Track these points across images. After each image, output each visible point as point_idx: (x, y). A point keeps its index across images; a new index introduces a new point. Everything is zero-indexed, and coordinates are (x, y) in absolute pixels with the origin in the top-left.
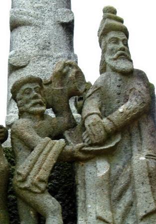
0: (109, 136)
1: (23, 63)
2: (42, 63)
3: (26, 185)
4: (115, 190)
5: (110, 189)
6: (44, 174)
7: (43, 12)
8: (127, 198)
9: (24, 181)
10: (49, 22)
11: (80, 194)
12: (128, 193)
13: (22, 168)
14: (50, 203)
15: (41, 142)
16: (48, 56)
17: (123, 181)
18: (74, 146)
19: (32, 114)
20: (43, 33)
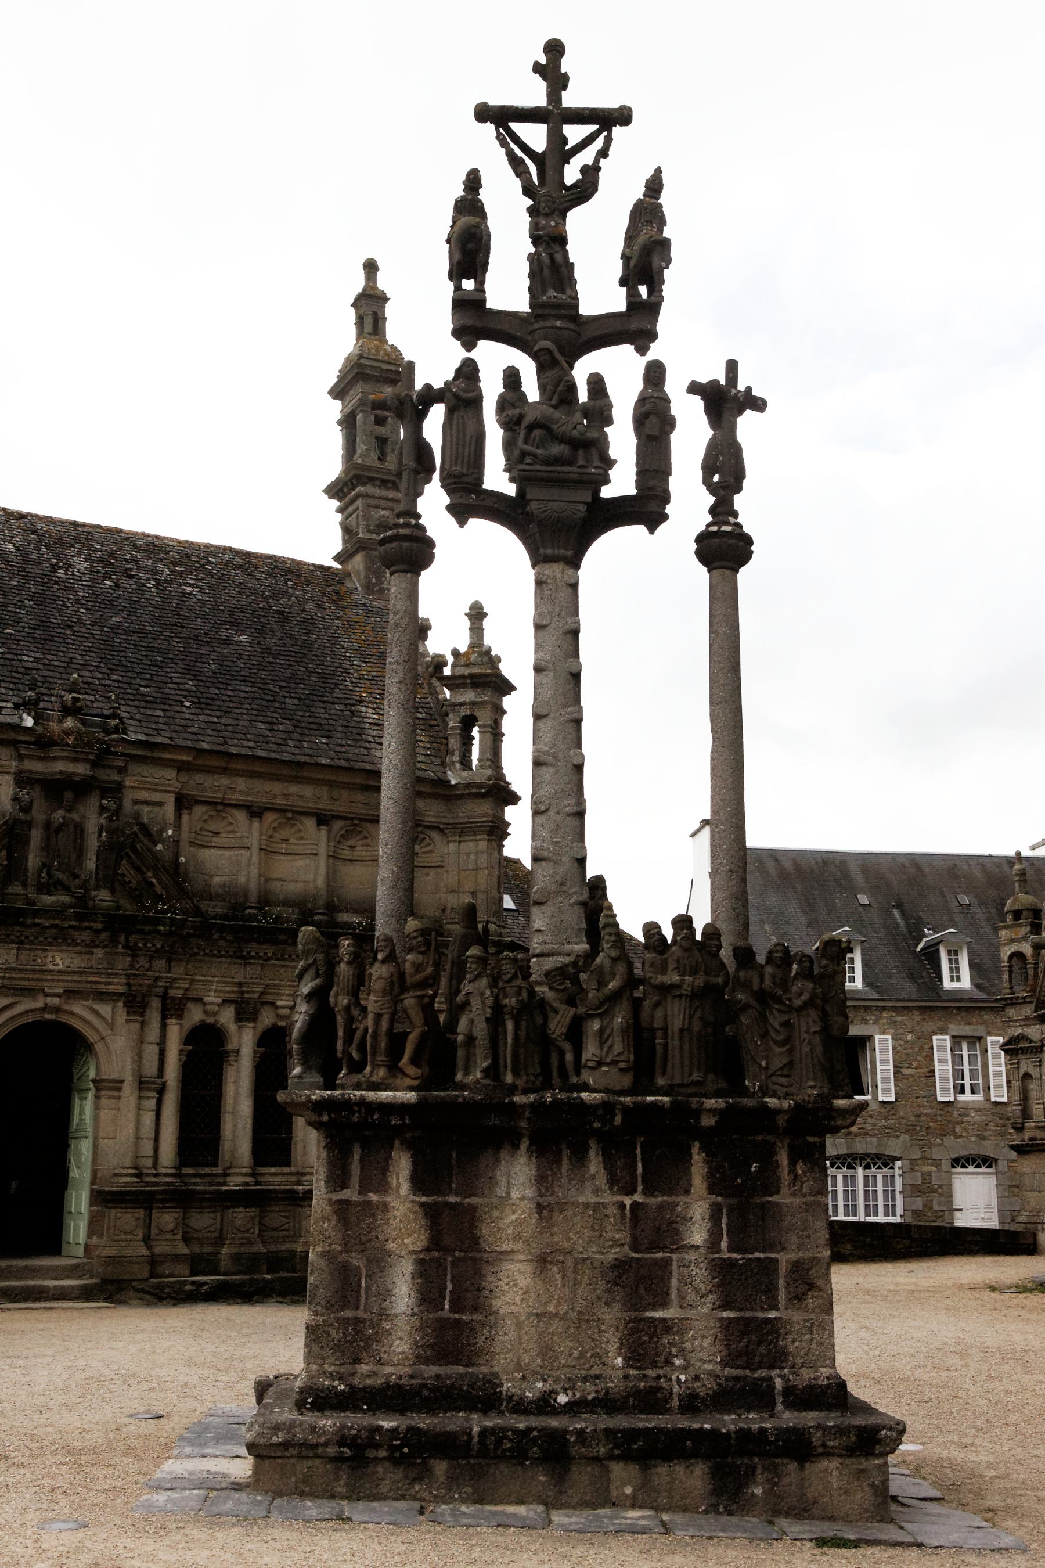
0: (601, 1004)
1: (545, 900)
2: (560, 899)
3: (554, 1036)
4: (602, 1036)
5: (601, 1037)
6: (564, 1030)
7: (561, 847)
8: (609, 1043)
9: (553, 1033)
10: (565, 859)
11: (584, 1038)
12: (611, 1039)
13: (552, 1026)
14: (567, 1046)
15: (562, 1008)
16: (564, 892)
17: (608, 1032)
18: (582, 1010)
19: (557, 991)
20: (561, 870)
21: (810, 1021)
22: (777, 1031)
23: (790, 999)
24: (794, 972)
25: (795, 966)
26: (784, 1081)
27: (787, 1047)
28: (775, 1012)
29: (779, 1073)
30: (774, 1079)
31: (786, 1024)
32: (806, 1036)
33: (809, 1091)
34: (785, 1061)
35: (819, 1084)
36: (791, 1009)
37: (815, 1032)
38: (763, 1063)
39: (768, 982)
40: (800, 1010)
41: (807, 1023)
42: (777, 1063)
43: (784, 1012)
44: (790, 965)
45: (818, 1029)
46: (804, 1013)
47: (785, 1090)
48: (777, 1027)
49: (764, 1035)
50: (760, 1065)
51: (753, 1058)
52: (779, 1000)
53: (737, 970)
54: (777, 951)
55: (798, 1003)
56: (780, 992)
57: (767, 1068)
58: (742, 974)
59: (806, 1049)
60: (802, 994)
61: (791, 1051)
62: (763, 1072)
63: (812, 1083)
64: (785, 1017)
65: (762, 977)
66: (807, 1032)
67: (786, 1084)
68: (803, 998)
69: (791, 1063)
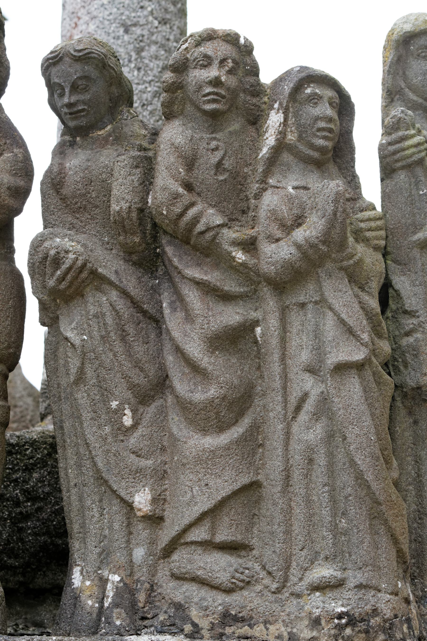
21: (329, 323)
22: (195, 368)
23: (250, 245)
24: (270, 139)
25: (275, 119)
26: (220, 566)
27: (237, 431)
28: (192, 296)
29: (199, 534)
30: (180, 559)
31: (234, 340)
32: (308, 383)
33: (316, 604)
34: (223, 485)
35: (354, 578)
36: (253, 282)
37: (341, 368)
38: (142, 500)
39: (167, 180)
40: (287, 282)
41: (317, 334)
42: (195, 495)
43: (226, 298)
44: (255, 121)
45: (359, 355)
46: (307, 293)
47: (218, 601)
48: (195, 349)
49: (154, 389)
50: (129, 506)
51: (101, 480)
52: (207, 250)
53: (60, 151)
54: (207, 61)
55: (278, 253)
56: (213, 217)
57: (155, 520)
58: (75, 162)
59: (309, 433)
60: (299, 221)
61: (252, 444)
62: (142, 532)
63: (324, 572)
64: (231, 316)
65: (147, 167)
66: (311, 370)
67: (223, 577)
68: (300, 234)
69: (251, 490)
